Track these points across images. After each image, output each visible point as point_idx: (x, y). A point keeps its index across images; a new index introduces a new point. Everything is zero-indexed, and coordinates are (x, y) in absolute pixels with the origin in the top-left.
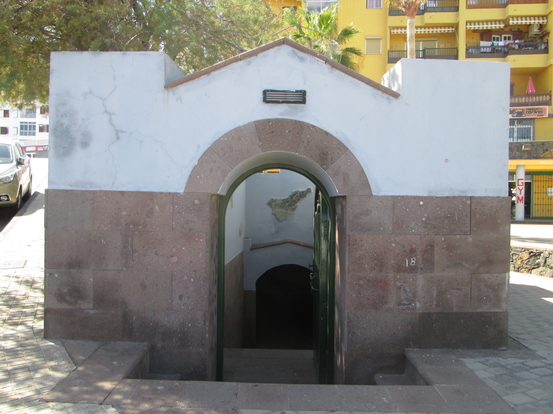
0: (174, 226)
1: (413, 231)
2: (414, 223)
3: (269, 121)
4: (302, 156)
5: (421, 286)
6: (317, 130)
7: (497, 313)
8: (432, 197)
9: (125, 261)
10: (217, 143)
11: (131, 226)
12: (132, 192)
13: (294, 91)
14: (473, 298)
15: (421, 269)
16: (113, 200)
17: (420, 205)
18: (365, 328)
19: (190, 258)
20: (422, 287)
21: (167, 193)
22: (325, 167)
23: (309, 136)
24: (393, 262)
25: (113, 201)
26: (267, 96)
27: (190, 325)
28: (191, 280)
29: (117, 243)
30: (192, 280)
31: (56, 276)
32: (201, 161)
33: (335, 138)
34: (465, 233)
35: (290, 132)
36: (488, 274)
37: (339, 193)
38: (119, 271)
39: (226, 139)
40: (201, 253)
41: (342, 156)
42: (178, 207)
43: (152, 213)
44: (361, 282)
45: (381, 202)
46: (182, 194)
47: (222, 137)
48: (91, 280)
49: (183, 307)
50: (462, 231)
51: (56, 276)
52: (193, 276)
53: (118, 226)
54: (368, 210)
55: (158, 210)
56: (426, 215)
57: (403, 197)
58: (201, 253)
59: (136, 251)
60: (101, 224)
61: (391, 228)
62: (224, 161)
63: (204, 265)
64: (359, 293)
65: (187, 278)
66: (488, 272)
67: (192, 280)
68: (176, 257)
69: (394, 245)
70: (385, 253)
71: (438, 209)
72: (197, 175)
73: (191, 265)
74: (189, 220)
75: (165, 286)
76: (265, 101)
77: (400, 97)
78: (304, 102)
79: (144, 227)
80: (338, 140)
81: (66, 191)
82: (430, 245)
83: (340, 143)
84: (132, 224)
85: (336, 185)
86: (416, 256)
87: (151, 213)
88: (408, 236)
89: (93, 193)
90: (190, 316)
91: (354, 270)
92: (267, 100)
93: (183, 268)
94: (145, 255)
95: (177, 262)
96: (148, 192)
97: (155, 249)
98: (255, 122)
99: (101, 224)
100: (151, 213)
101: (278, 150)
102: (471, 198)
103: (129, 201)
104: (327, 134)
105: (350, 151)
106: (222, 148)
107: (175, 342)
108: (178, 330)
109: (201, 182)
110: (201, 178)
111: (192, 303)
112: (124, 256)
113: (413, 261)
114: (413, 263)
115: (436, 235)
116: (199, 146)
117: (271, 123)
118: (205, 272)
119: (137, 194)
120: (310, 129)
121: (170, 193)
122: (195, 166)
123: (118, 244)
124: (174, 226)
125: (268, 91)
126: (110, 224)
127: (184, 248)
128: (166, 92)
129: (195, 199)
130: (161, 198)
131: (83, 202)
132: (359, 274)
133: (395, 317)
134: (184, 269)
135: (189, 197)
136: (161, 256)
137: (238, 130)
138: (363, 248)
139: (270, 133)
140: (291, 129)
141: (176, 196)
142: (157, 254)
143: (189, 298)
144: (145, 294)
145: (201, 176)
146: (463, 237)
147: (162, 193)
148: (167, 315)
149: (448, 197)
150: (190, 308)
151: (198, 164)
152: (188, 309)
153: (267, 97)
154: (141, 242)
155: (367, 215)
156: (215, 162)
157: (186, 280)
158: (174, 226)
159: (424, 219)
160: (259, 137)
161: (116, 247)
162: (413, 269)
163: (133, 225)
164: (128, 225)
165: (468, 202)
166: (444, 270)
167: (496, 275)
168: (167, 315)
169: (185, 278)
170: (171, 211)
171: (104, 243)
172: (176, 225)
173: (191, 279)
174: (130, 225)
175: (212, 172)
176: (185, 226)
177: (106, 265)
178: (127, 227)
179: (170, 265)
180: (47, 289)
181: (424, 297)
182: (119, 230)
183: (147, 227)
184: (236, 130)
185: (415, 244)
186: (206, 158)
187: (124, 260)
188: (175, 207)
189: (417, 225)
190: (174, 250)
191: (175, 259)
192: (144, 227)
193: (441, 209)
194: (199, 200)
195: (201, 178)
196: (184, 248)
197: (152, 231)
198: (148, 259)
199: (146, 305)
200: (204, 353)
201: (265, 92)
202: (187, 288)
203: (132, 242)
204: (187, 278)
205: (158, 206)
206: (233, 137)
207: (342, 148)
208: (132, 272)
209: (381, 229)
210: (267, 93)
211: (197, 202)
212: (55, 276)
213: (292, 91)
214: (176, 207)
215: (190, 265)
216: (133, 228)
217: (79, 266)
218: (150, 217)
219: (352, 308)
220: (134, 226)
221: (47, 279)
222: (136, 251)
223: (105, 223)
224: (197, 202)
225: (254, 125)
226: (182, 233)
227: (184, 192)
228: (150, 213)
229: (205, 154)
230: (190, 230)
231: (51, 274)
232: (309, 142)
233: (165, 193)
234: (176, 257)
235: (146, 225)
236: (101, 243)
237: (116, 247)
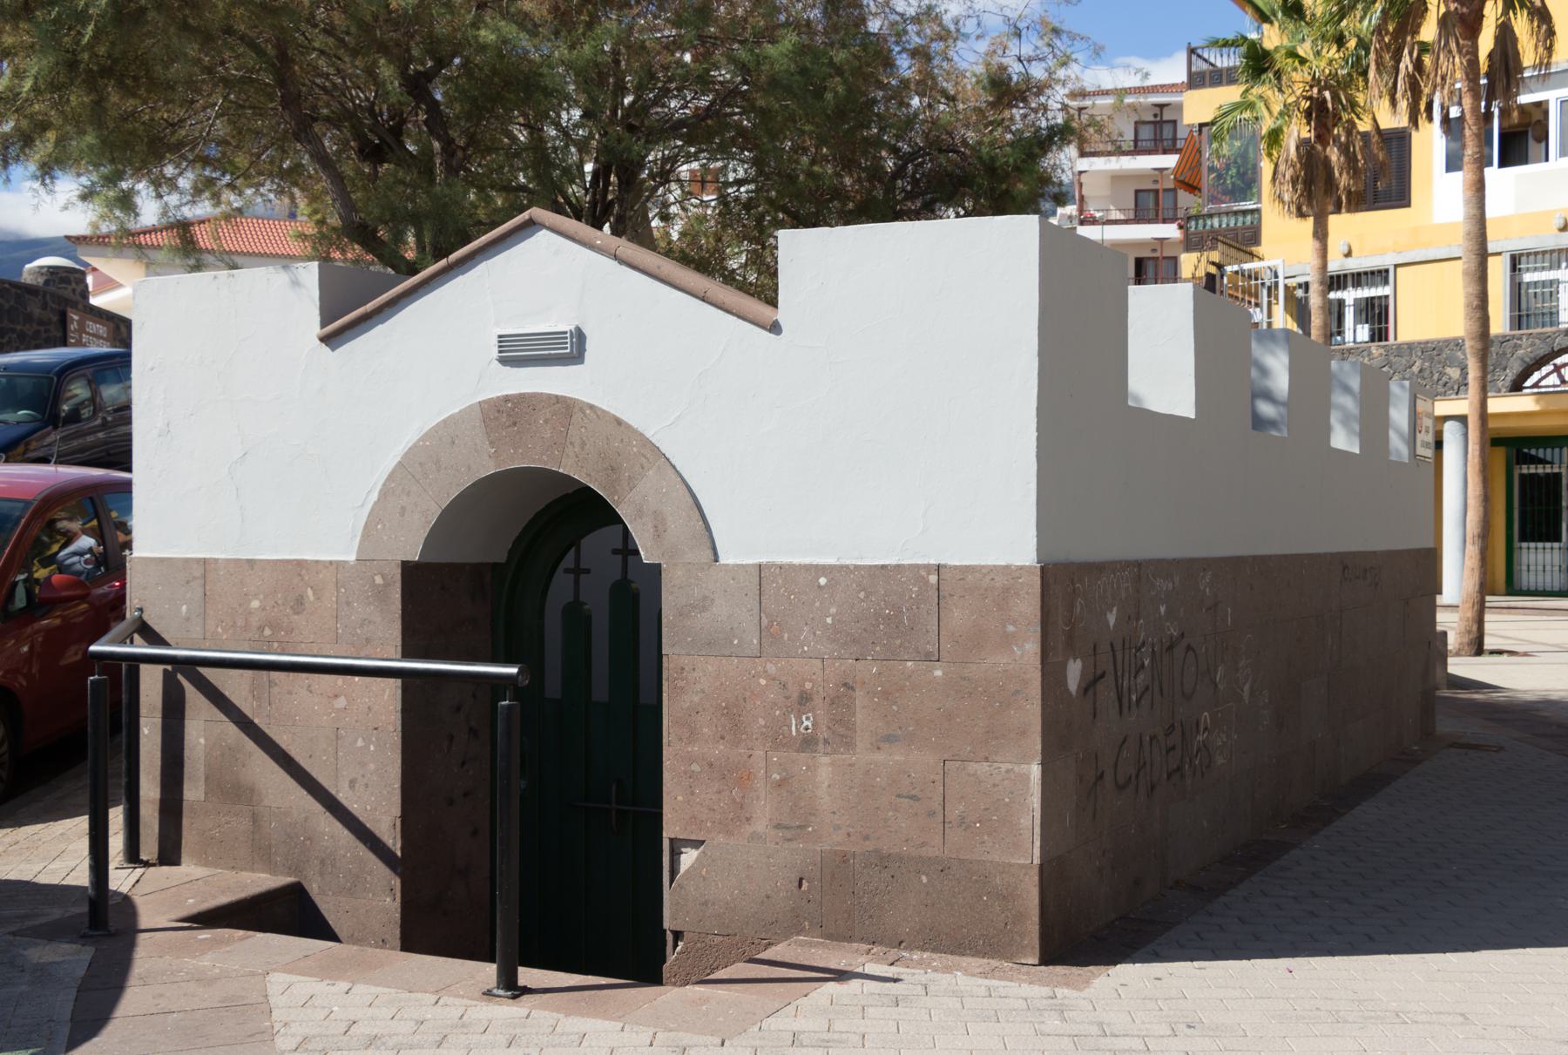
1: (806, 648)
5: (826, 784)
8: (847, 567)
11: (267, 632)
14: (950, 822)
15: (826, 741)
17: (819, 587)
18: (704, 879)
20: (829, 786)
23: (583, 430)
24: (762, 722)
30: (372, 748)
32: (384, 493)
34: (928, 658)
35: (546, 421)
44: (695, 767)
45: (733, 579)
48: (202, 741)
50: (919, 652)
54: (705, 598)
55: (312, 598)
56: (833, 610)
61: (755, 642)
64: (693, 794)
66: (987, 760)
67: (372, 748)
68: (343, 697)
69: (763, 682)
71: (862, 595)
82: (845, 685)
86: (813, 710)
88: (794, 660)
93: (356, 721)
94: (290, 693)
102: (938, 568)
113: (806, 723)
114: (807, 729)
120: (584, 413)
124: (340, 631)
132: (690, 749)
133: (769, 857)
138: (698, 687)
139: (509, 426)
142: (311, 692)
143: (367, 786)
146: (923, 665)
150: (369, 808)
155: (704, 609)
159: (829, 620)
162: (808, 743)
165: (933, 579)
169: (360, 743)
170: (334, 599)
176: (359, 631)
181: (834, 813)
189: (814, 634)
193: (867, 597)
202: (363, 764)
206: (440, 439)
209: (736, 642)
211: (379, 580)
214: (343, 590)
218: (298, 613)
219: (678, 828)
222: (276, 684)
228: (299, 604)
229: (391, 477)
232: (583, 444)
234: (343, 697)
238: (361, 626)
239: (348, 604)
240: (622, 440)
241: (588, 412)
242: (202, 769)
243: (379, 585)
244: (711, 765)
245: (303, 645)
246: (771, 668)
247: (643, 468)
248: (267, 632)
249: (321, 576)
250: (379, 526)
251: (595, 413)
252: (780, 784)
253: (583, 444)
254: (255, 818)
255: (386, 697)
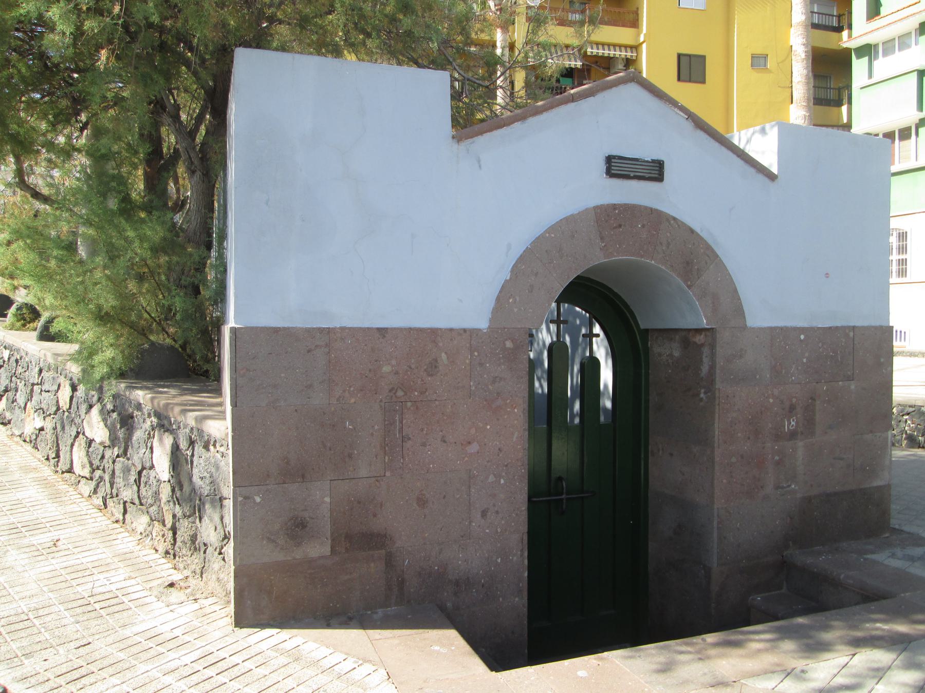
0: (473, 388)
2: (794, 366)
3: (614, 207)
4: (660, 266)
5: (801, 459)
6: (679, 226)
7: (880, 487)
9: (389, 459)
10: (539, 241)
11: (400, 393)
12: (401, 330)
13: (649, 159)
16: (366, 345)
17: (801, 341)
19: (498, 443)
20: (803, 459)
21: (461, 329)
22: (689, 283)
23: (669, 234)
24: (770, 425)
25: (366, 348)
26: (613, 166)
27: (499, 560)
28: (500, 482)
29: (373, 426)
31: (258, 499)
32: (515, 270)
33: (702, 238)
35: (643, 226)
36: (870, 435)
37: (707, 324)
38: (379, 478)
39: (553, 235)
40: (517, 433)
41: (711, 267)
42: (479, 355)
43: (436, 367)
44: (734, 460)
46: (485, 331)
47: (546, 231)
48: (327, 499)
49: (487, 531)
51: (258, 499)
52: (504, 474)
53: (376, 393)
55: (446, 362)
56: (807, 355)
57: (781, 328)
58: (517, 433)
59: (409, 439)
60: (344, 391)
61: (768, 376)
62: (550, 272)
63: (521, 454)
64: (732, 477)
65: (495, 479)
66: (871, 432)
67: (502, 481)
68: (475, 443)
69: (771, 400)
70: (761, 412)
71: (820, 345)
72: (510, 298)
73: (501, 455)
74: (496, 377)
75: (458, 496)
76: (610, 173)
77: (776, 181)
78: (659, 178)
79: (422, 393)
80: (706, 241)
81: (276, 330)
83: (708, 247)
84: (400, 388)
85: (704, 312)
87: (433, 367)
89: (329, 332)
90: (499, 545)
91: (725, 442)
92: (613, 172)
93: (488, 462)
95: (478, 452)
96: (429, 329)
97: (442, 432)
98: (596, 208)
99: (344, 391)
100: (433, 367)
101: (626, 256)
102: (854, 327)
103: (396, 347)
104: (692, 231)
105: (720, 260)
106: (546, 251)
107: (475, 594)
108: (481, 572)
109: (516, 310)
110: (515, 301)
111: (503, 522)
112: (387, 448)
113: (792, 423)
114: (793, 425)
115: (817, 383)
116: (509, 247)
117: (617, 211)
118: (523, 465)
119: (410, 332)
121: (465, 330)
122: (506, 281)
123: (376, 427)
125: (614, 157)
126: (361, 390)
127: (488, 427)
128: (456, 146)
129: (506, 340)
130: (451, 340)
131: (309, 351)
132: (730, 448)
134: (489, 464)
135: (496, 336)
136: (451, 443)
137: (569, 220)
140: (645, 223)
141: (475, 335)
142: (445, 441)
143: (497, 512)
144: (425, 516)
145: (516, 299)
147: (451, 330)
148: (462, 548)
149: (830, 328)
150: (499, 530)
151: (511, 278)
152: (497, 532)
153: (613, 168)
154: (417, 420)
155: (741, 357)
156: (536, 274)
157: (492, 482)
158: (473, 388)
159: (805, 360)
160: (601, 233)
161: (372, 434)
162: (793, 435)
163: (402, 390)
164: (394, 391)
165: (851, 334)
166: (826, 433)
167: (879, 434)
168: (462, 548)
169: (491, 478)
170: (467, 361)
171: (350, 427)
172: (476, 388)
173: (500, 479)
174: (396, 391)
175: (532, 291)
176: (490, 387)
177: (355, 469)
178: (392, 394)
179: (466, 459)
180: (238, 528)
182: (378, 401)
183: (427, 394)
184: (567, 219)
185: (795, 397)
186: (524, 267)
187: (387, 458)
188: (474, 355)
190: (473, 431)
191: (474, 448)
192: (422, 393)
194: (512, 341)
195: (515, 302)
196: (488, 427)
197: (436, 400)
198: (429, 451)
199: (426, 535)
200: (521, 606)
201: (609, 159)
203: (401, 422)
204: (495, 479)
205: (446, 353)
207: (710, 254)
208: (402, 478)
209: (758, 377)
210: (613, 160)
211: (509, 344)
212: (254, 500)
213: (646, 159)
214: (476, 354)
215: (498, 455)
216: (404, 396)
217: (303, 476)
218: (432, 375)
219: (723, 501)
220: (405, 392)
221: (239, 507)
222: (409, 439)
223: (352, 389)
224: (509, 344)
225: (593, 212)
226: (486, 400)
227: (489, 327)
228: (433, 367)
230: (498, 394)
231: (246, 498)
232: (669, 244)
233: (457, 330)
234: (475, 443)
235: (426, 389)
236: (345, 427)
237: (372, 434)
238: (494, 382)
239: (481, 364)
240: (694, 243)
241: (672, 222)
242: (328, 527)
243: (510, 349)
244: (742, 457)
245: (437, 403)
246: (776, 392)
247: (706, 263)
248: (400, 393)
249: (455, 342)
250: (511, 301)
251: (677, 224)
252: (778, 463)
253: (669, 244)
254: (389, 561)
255: (514, 439)
